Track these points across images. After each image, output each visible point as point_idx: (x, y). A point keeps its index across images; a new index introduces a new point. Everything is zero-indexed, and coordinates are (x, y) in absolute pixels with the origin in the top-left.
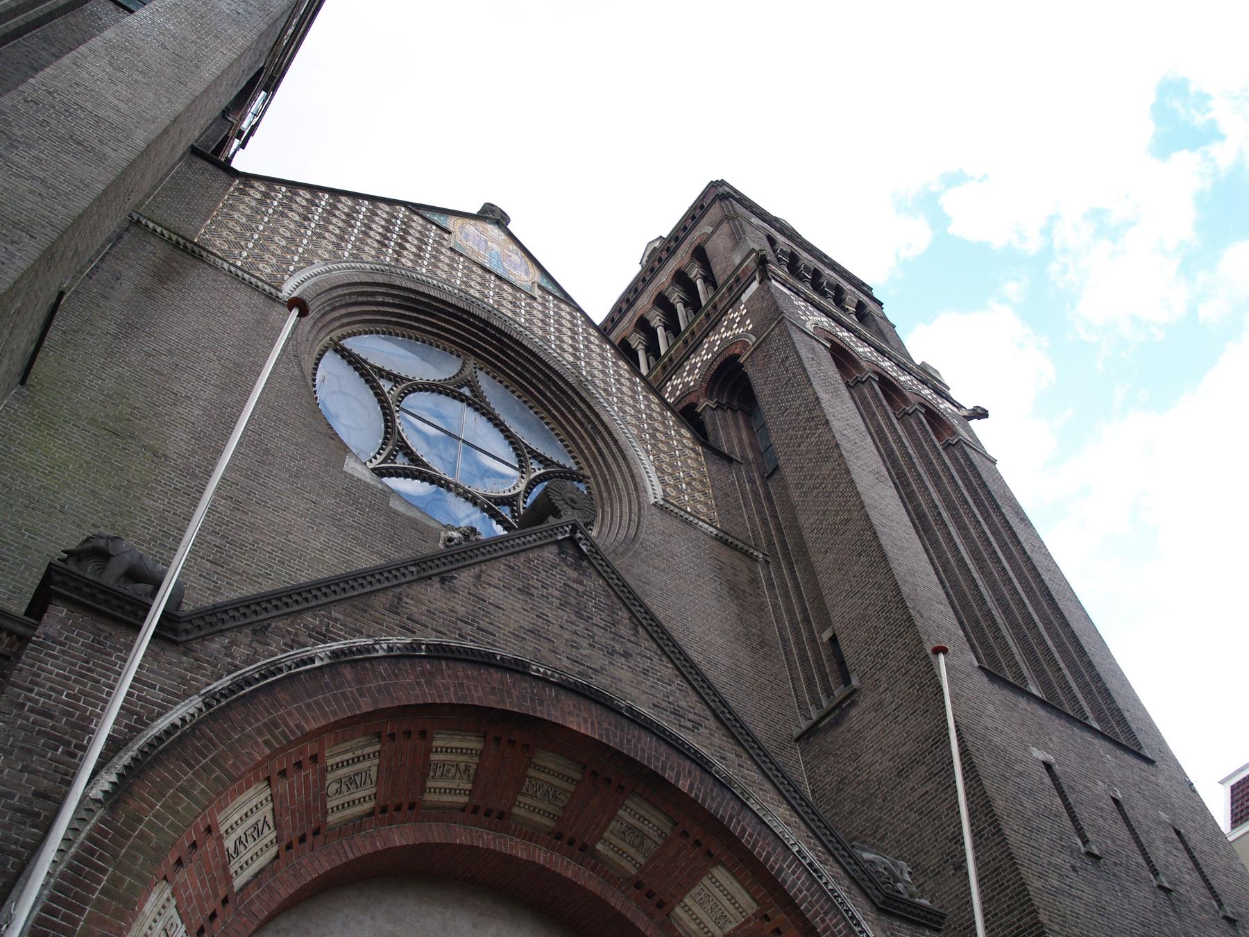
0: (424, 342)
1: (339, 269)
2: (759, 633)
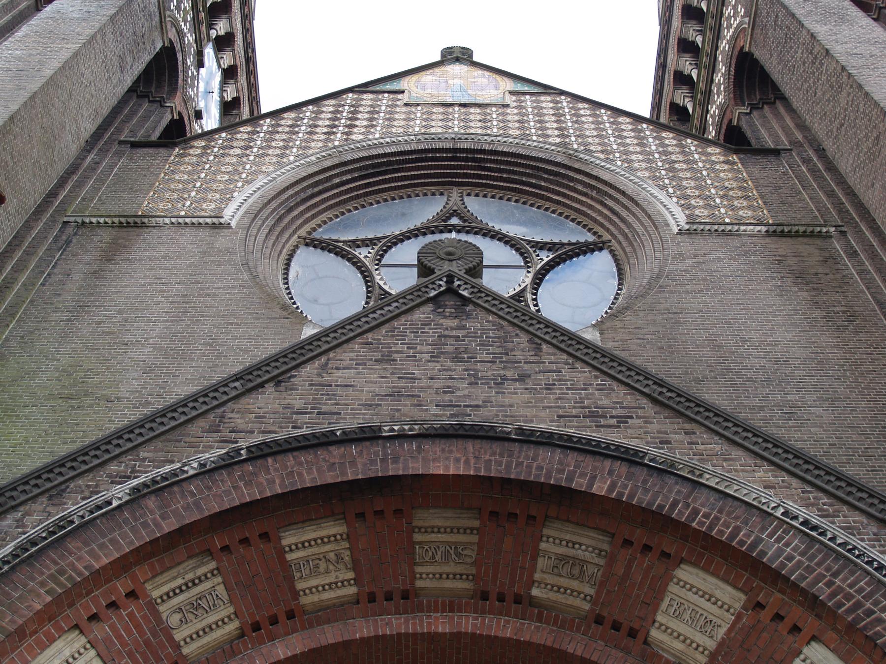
0: (401, 198)
1: (284, 173)
2: (843, 308)
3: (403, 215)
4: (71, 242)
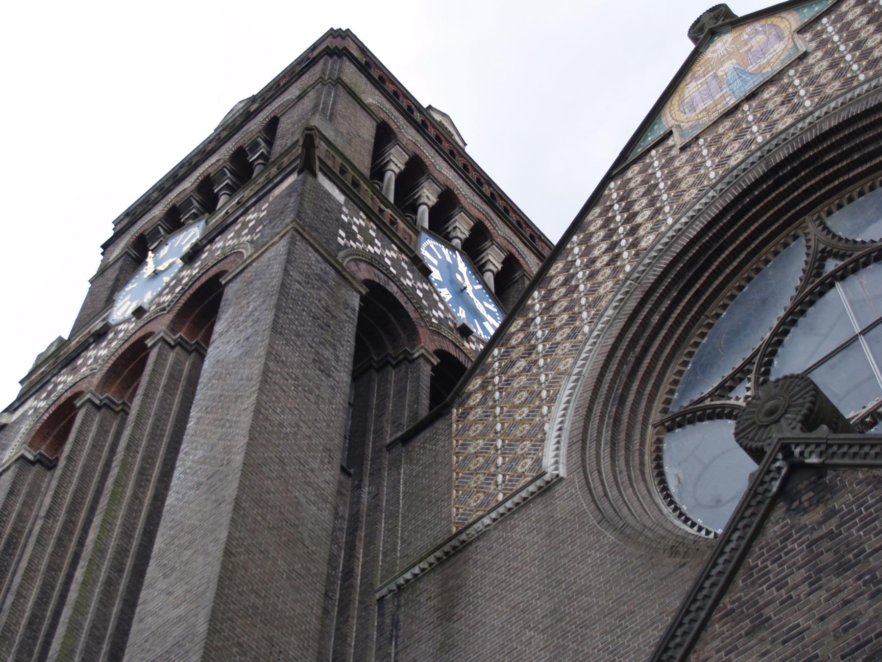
0: (749, 279)
1: (586, 359)
3: (764, 301)
4: (398, 621)
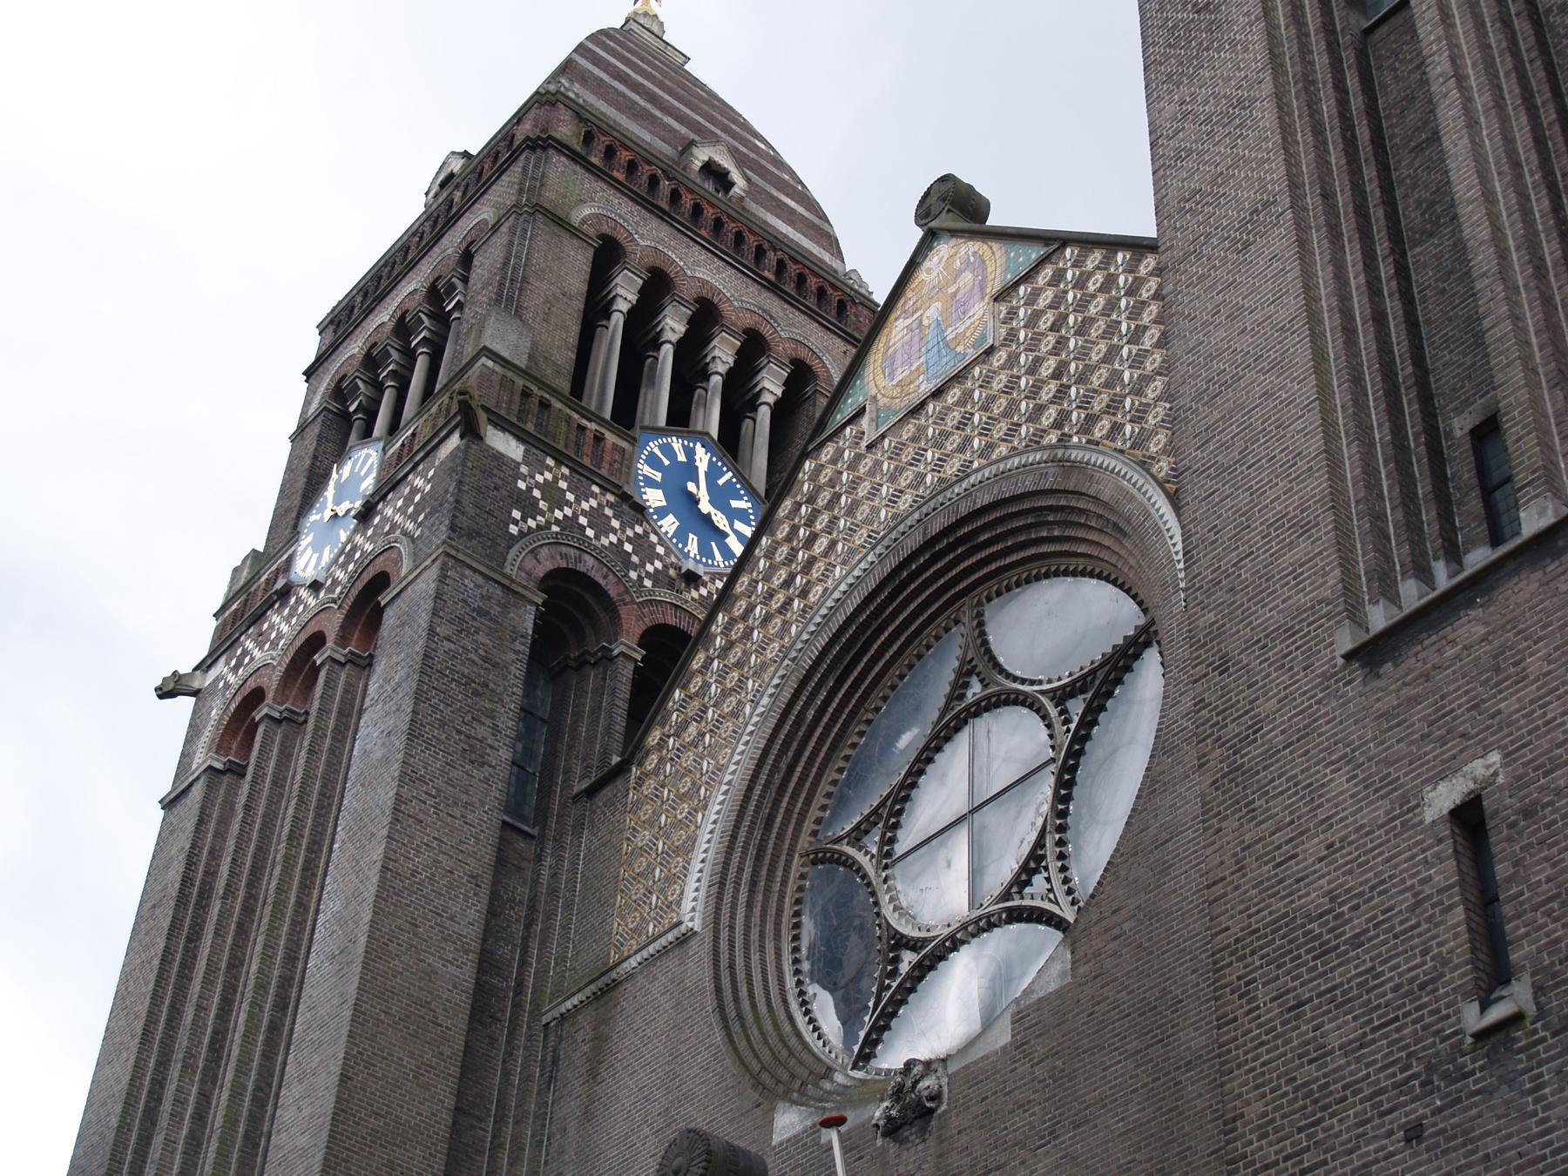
4: (559, 1060)
